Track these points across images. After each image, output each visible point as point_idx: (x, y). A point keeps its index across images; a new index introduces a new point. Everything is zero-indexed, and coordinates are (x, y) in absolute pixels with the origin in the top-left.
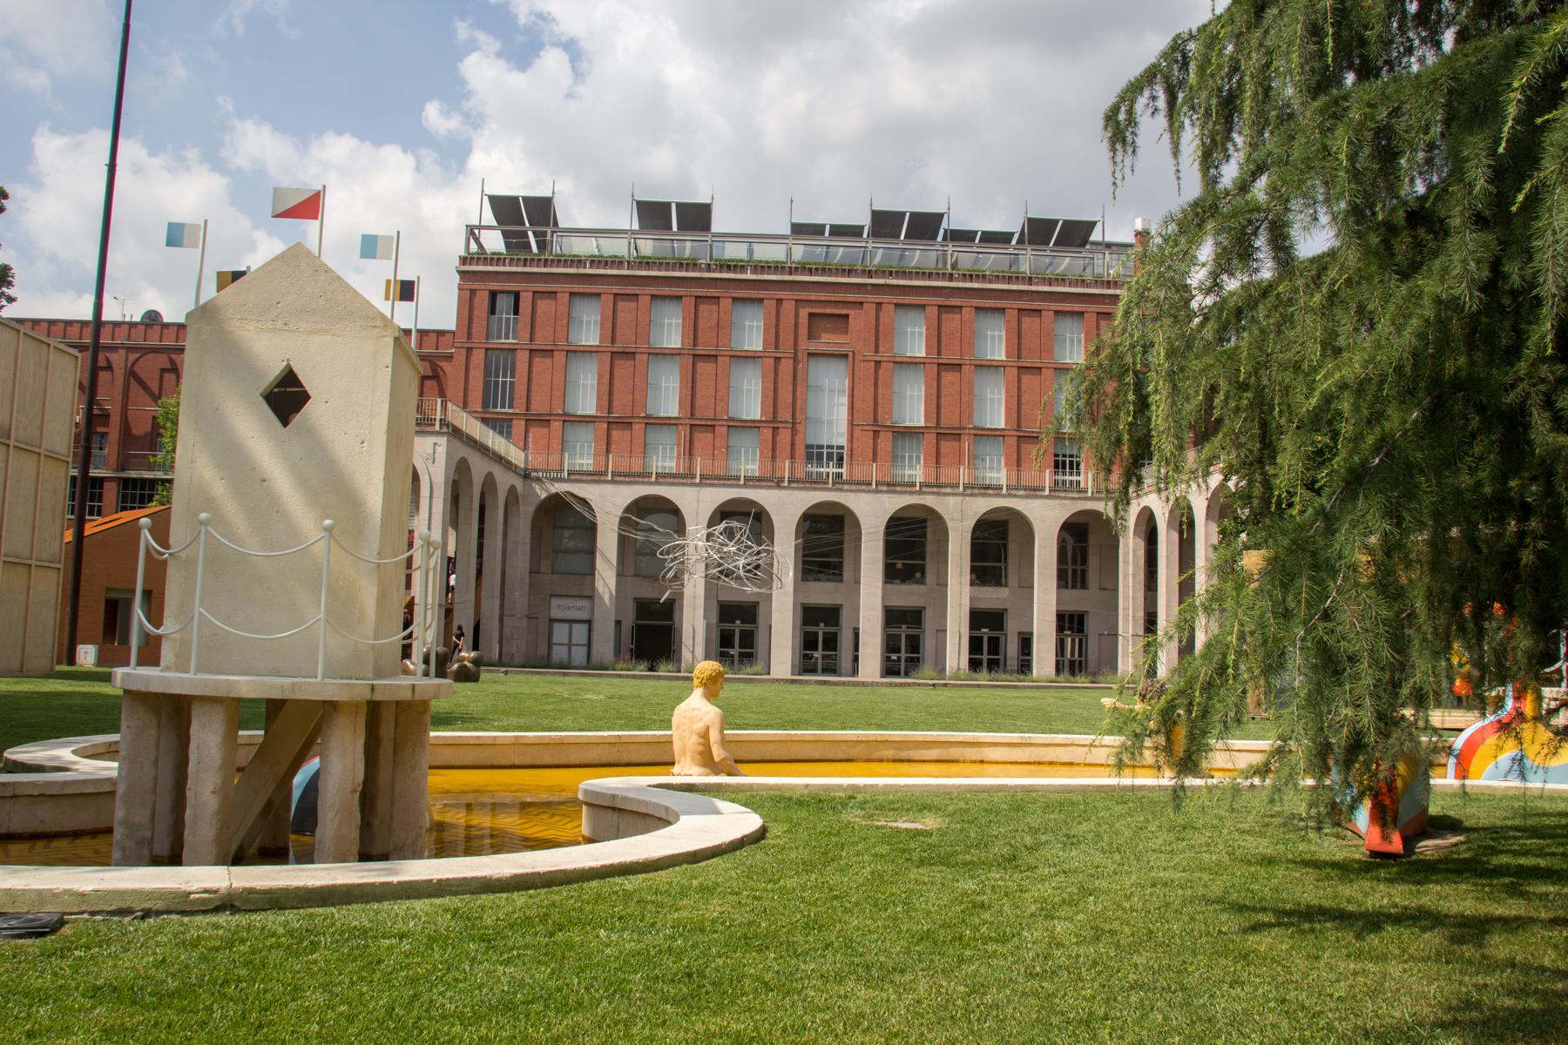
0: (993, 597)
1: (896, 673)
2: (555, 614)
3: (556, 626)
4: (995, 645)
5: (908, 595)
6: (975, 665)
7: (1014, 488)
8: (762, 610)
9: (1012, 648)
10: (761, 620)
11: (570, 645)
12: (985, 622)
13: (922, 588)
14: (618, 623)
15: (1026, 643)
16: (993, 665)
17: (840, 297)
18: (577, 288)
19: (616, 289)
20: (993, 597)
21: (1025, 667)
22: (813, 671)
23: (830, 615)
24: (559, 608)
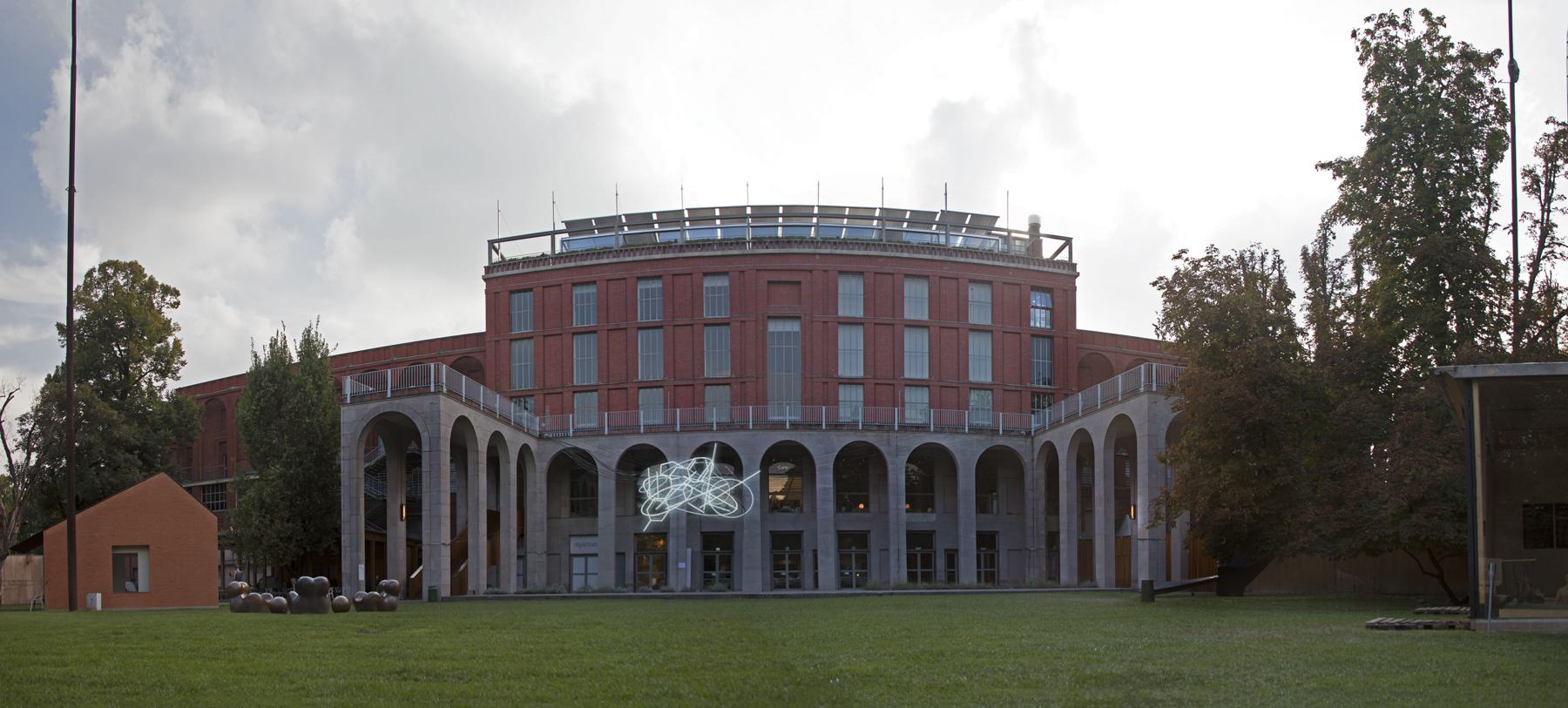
0: (925, 520)
1: (850, 586)
2: (574, 550)
3: (575, 560)
4: (928, 561)
5: (852, 522)
6: (912, 577)
7: (940, 430)
8: (736, 537)
9: (941, 563)
10: (736, 547)
11: (586, 574)
12: (919, 540)
13: (867, 515)
14: (620, 555)
15: (952, 557)
16: (927, 577)
17: (794, 264)
18: (577, 278)
19: (609, 275)
20: (925, 520)
21: (952, 578)
22: (782, 586)
23: (794, 539)
24: (575, 546)
